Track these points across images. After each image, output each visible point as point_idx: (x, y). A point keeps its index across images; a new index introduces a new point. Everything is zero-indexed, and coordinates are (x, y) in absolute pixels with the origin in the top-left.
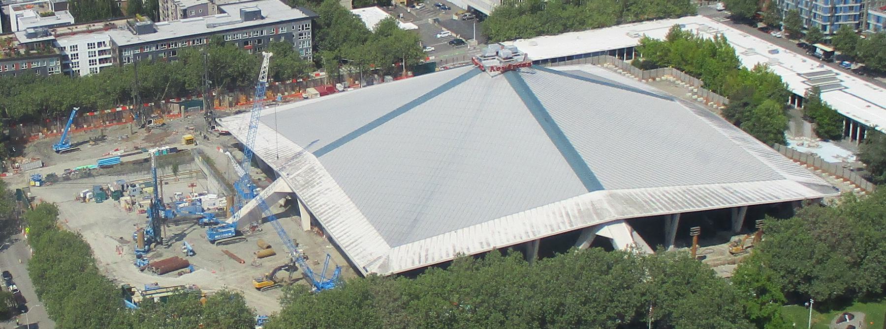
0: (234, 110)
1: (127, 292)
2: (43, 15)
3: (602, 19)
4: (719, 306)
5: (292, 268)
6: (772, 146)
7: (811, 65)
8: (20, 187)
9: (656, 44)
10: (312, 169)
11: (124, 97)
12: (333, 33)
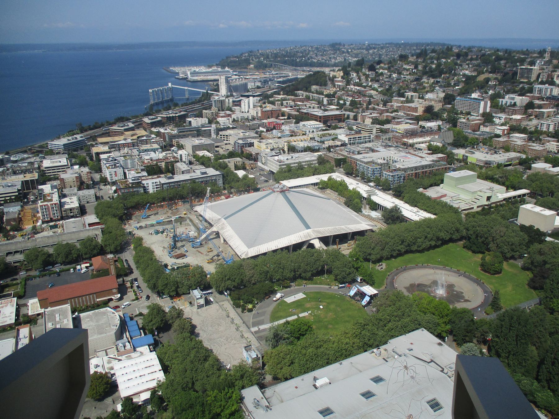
0: (199, 203)
1: (166, 266)
2: (137, 173)
3: (309, 174)
4: (346, 265)
5: (218, 256)
6: (358, 213)
7: (367, 188)
8: (131, 230)
9: (325, 181)
10: (224, 224)
11: (164, 200)
12: (229, 179)
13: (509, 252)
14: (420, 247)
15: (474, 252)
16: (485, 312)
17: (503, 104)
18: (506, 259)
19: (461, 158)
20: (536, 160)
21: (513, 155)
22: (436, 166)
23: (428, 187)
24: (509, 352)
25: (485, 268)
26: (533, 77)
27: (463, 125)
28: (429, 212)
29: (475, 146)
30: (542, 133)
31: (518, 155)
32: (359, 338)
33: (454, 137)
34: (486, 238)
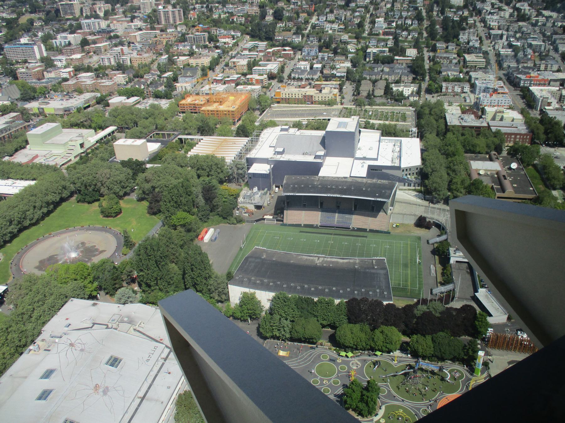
13: (120, 190)
14: (32, 219)
15: (89, 203)
16: (123, 254)
17: (58, 45)
18: (121, 197)
19: (37, 111)
20: (110, 95)
21: (88, 96)
22: (13, 128)
23: (14, 153)
24: (156, 279)
25: (107, 214)
26: (78, 14)
27: (24, 76)
28: (26, 180)
29: (47, 96)
30: (105, 68)
31: (93, 94)
32: (8, 346)
33: (20, 90)
34: (96, 185)
